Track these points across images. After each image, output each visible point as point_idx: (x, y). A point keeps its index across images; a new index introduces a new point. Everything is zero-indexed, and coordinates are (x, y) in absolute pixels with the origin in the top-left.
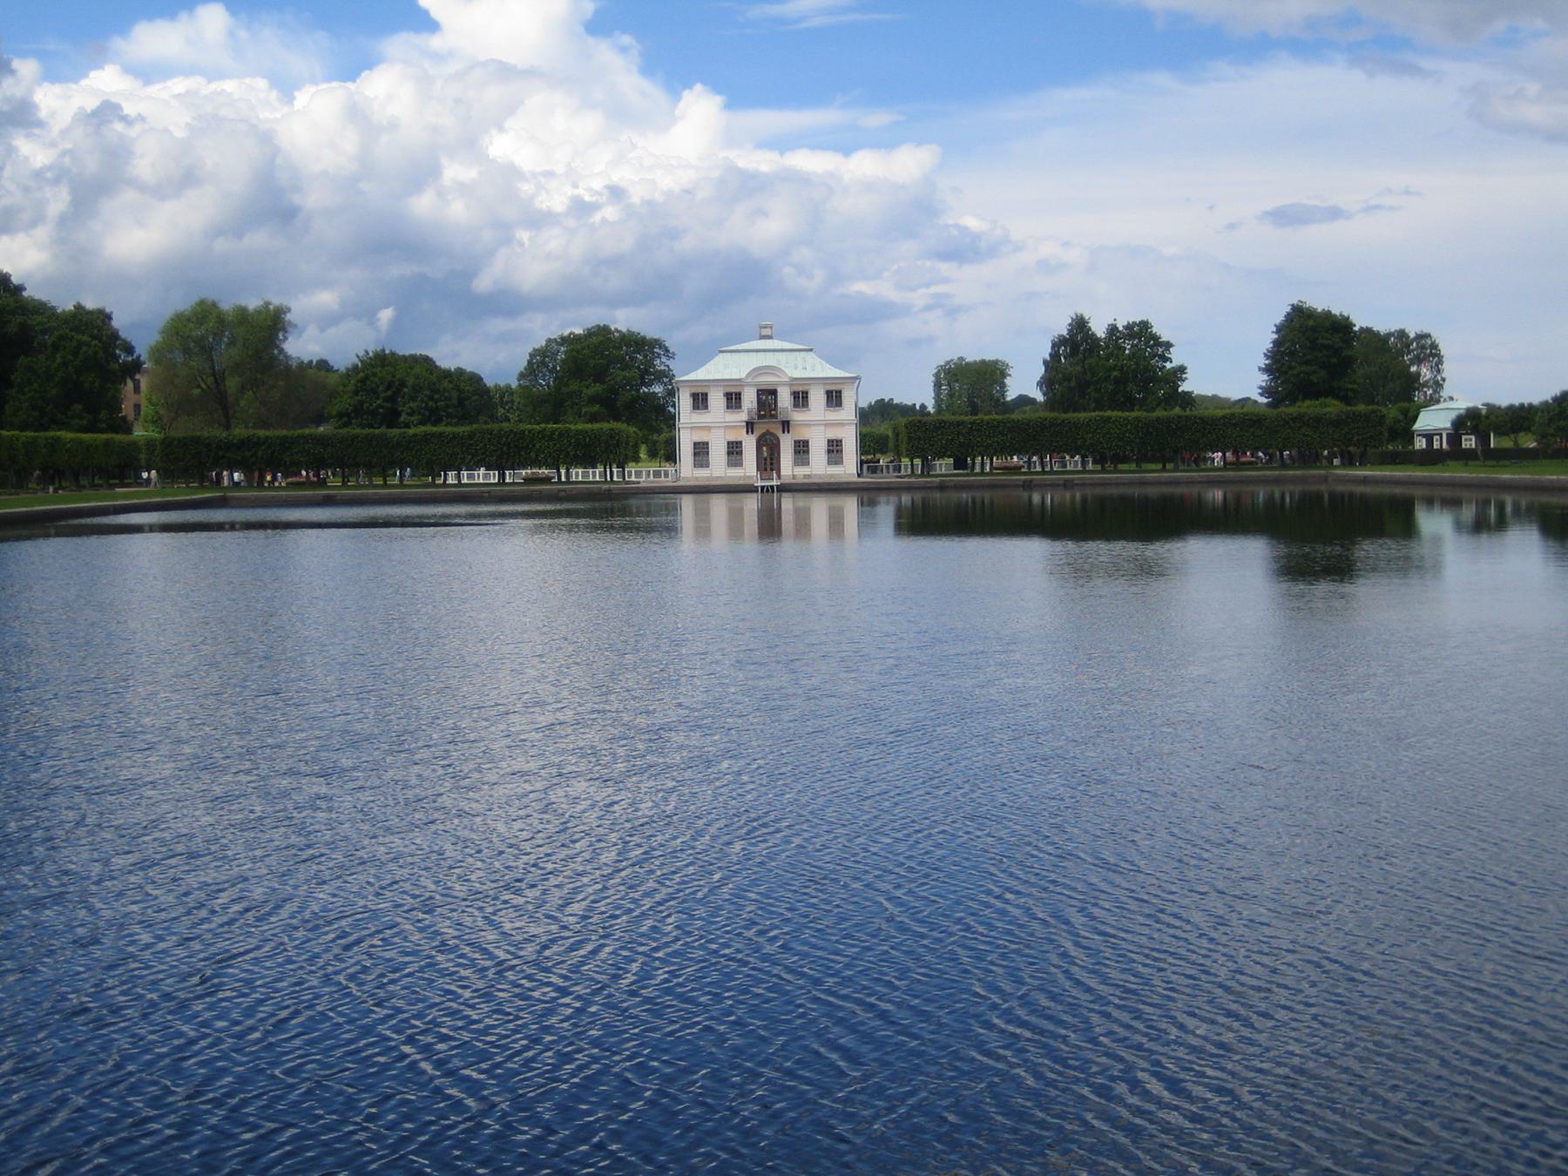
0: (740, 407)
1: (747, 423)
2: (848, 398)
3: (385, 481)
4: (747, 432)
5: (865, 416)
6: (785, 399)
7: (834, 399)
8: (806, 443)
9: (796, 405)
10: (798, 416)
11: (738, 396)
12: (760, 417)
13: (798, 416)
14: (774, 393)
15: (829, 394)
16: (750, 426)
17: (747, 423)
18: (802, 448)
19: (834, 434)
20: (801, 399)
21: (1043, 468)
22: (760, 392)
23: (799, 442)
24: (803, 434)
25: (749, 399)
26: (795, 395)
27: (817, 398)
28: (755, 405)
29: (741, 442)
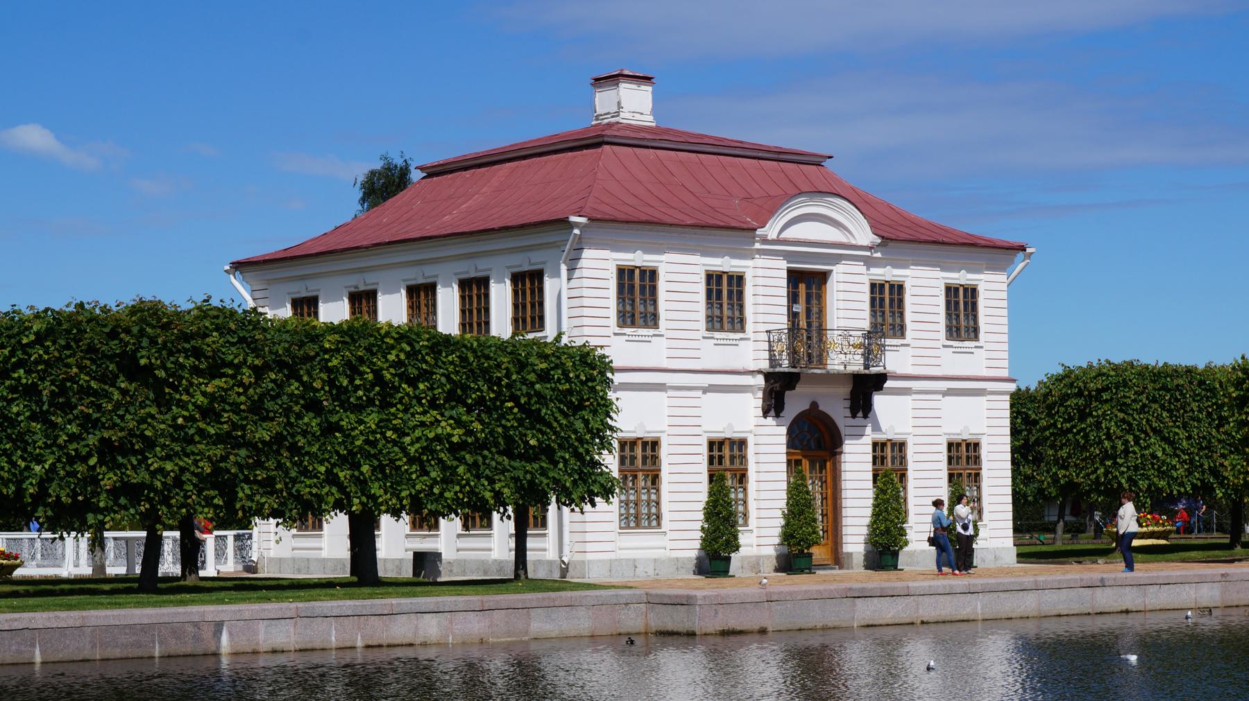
0: (738, 323)
13: (895, 359)
14: (821, 278)
17: (768, 376)
22: (795, 277)
29: (742, 443)
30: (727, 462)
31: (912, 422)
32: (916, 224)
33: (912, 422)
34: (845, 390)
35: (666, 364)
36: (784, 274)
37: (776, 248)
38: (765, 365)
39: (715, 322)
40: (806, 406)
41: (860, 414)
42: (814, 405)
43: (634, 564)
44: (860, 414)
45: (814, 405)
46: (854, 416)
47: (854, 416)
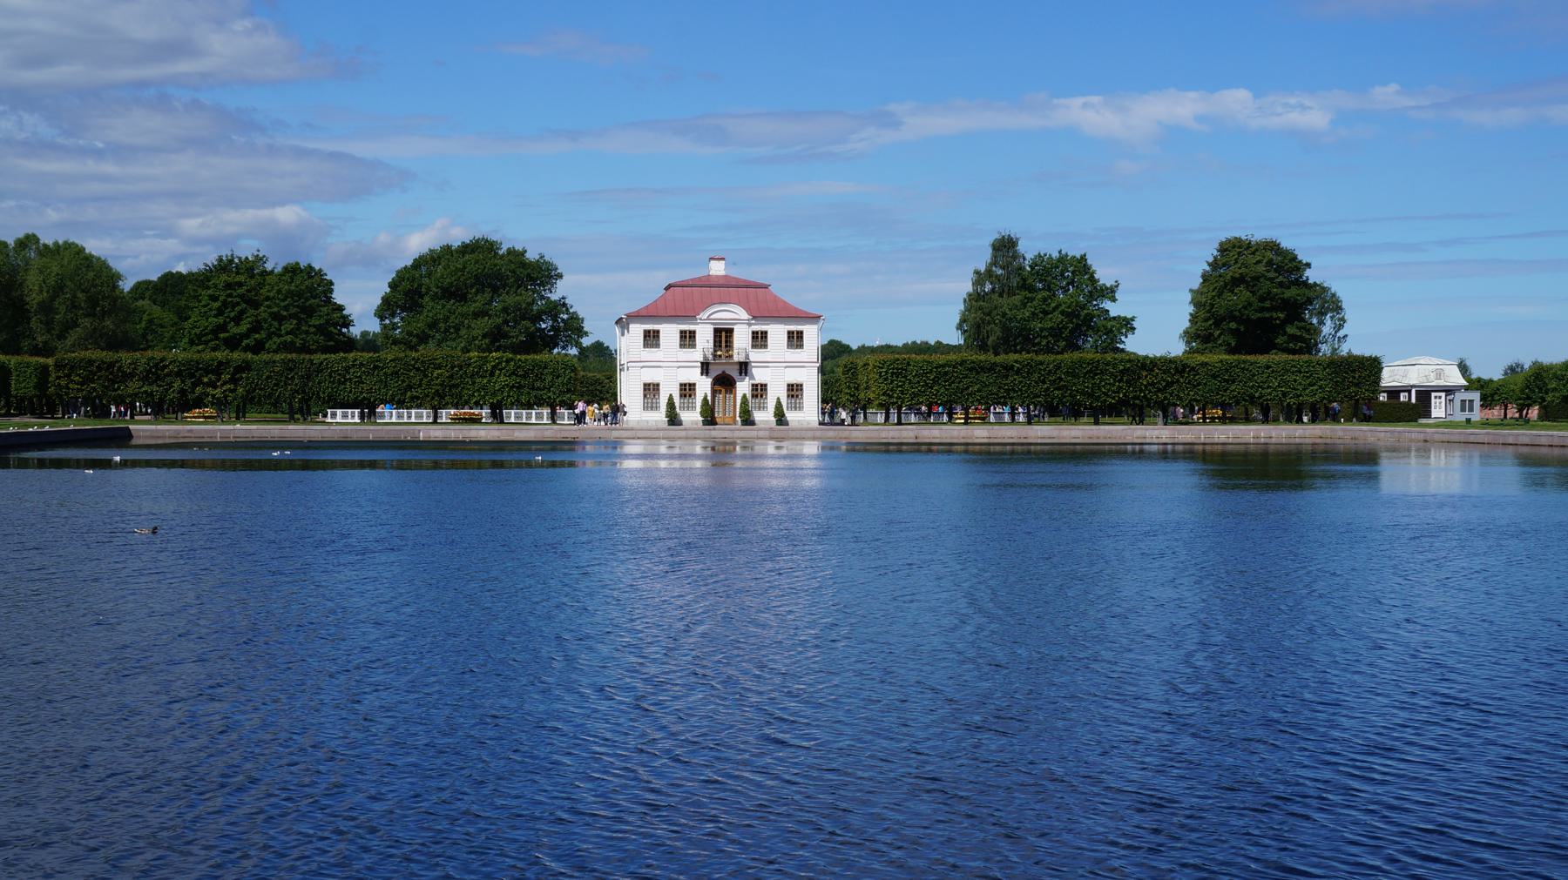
0: (693, 346)
4: (702, 374)
5: (832, 352)
6: (742, 339)
7: (795, 339)
8: (764, 387)
9: (754, 346)
10: (755, 356)
11: (692, 334)
12: (715, 356)
13: (755, 356)
14: (730, 332)
16: (705, 368)
17: (702, 363)
18: (760, 390)
19: (794, 376)
20: (759, 339)
22: (717, 332)
24: (759, 375)
26: (755, 335)
28: (711, 344)
32: (797, 310)
34: (737, 367)
36: (712, 330)
37: (706, 321)
38: (702, 360)
39: (682, 346)
40: (720, 372)
42: (724, 372)
43: (648, 422)
45: (724, 372)
46: (741, 374)
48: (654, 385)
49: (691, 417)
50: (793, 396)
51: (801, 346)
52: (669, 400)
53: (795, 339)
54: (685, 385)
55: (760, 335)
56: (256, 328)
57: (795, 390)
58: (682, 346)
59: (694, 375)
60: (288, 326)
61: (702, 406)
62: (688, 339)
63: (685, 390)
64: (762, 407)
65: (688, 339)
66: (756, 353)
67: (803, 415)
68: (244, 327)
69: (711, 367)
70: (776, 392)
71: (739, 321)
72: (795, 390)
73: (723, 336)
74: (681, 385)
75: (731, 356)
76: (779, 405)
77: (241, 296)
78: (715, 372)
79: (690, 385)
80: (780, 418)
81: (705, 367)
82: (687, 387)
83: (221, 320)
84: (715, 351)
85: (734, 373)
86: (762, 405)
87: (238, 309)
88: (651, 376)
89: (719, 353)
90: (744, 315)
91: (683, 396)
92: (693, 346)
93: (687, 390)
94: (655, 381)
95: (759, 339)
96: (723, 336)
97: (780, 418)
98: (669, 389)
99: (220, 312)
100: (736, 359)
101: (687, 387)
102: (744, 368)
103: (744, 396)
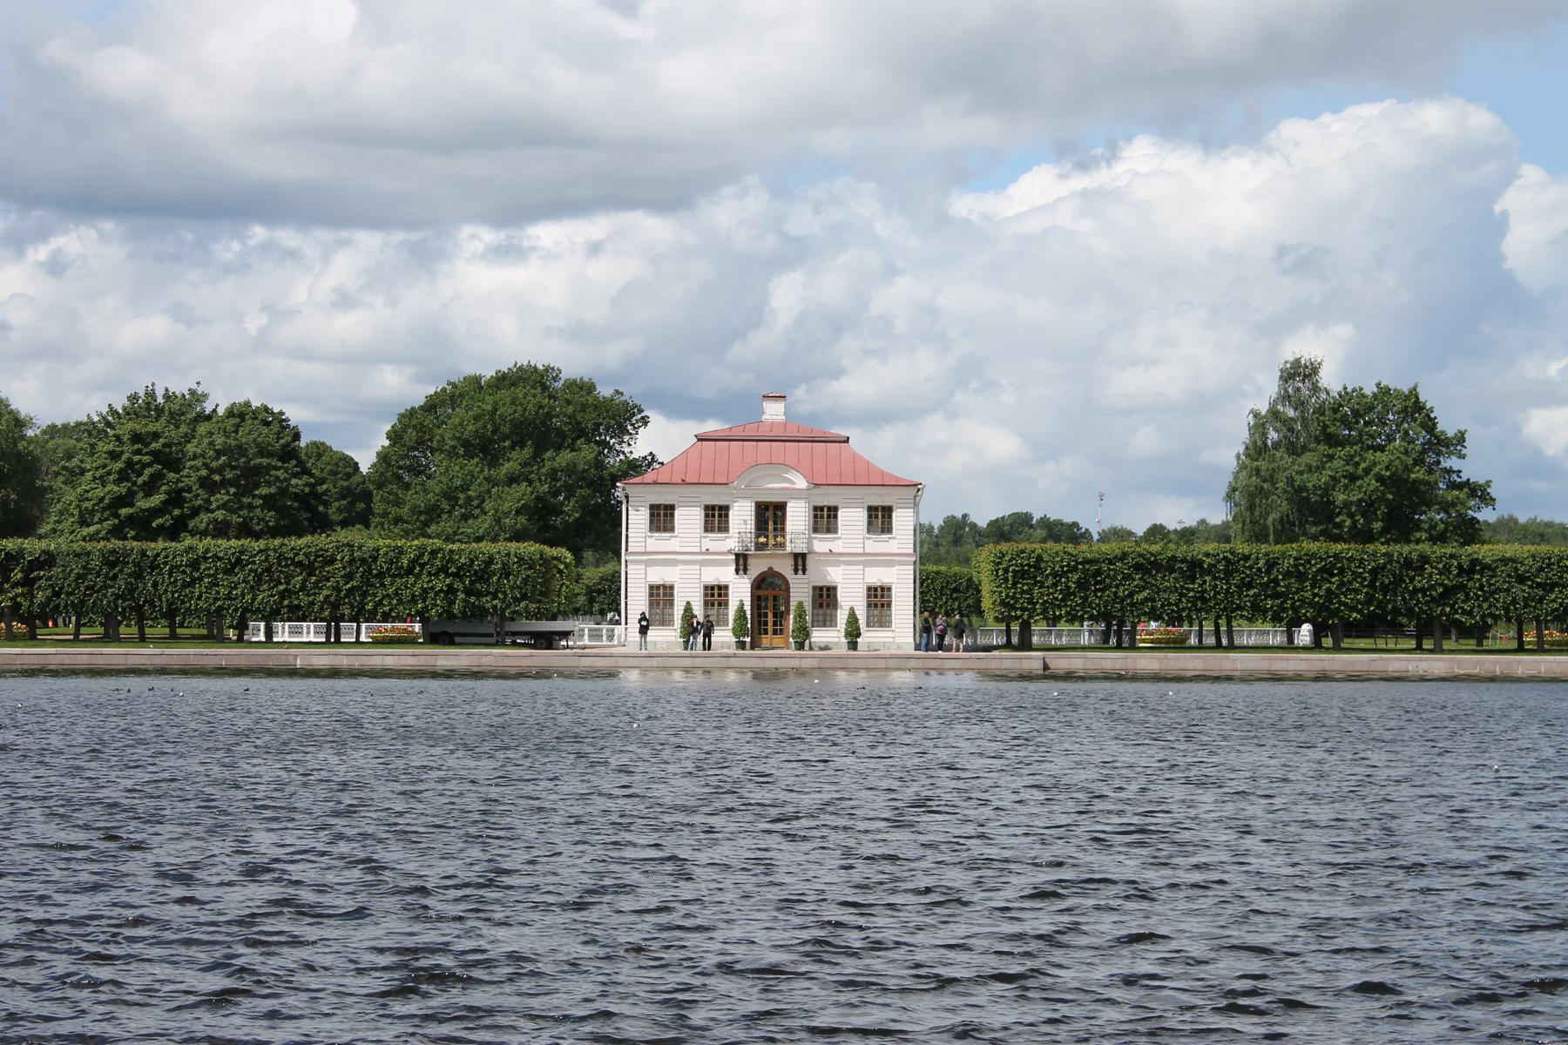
0: (726, 530)
1: (737, 555)
2: (903, 521)
3: (172, 627)
4: (737, 571)
6: (797, 518)
7: (880, 518)
11: (723, 511)
12: (760, 547)
14: (780, 508)
15: (872, 511)
16: (741, 562)
17: (737, 555)
18: (825, 597)
19: (877, 576)
20: (824, 518)
21: (1200, 641)
23: (821, 588)
25: (742, 516)
26: (817, 509)
27: (852, 519)
30: (716, 597)
31: (841, 576)
33: (841, 576)
35: (678, 550)
36: (753, 504)
39: (708, 528)
41: (800, 572)
42: (770, 568)
44: (800, 572)
45: (770, 568)
46: (796, 573)
47: (796, 573)
48: (665, 587)
49: (723, 636)
50: (876, 606)
51: (887, 528)
52: (685, 610)
53: (880, 518)
54: (712, 588)
55: (825, 513)
56: (176, 499)
57: (879, 598)
58: (708, 528)
59: (725, 574)
60: (221, 497)
61: (735, 620)
62: (716, 518)
63: (713, 595)
64: (828, 621)
65: (716, 518)
66: (821, 540)
67: (890, 634)
68: (156, 500)
69: (750, 561)
70: (851, 599)
71: (797, 494)
72: (879, 598)
73: (770, 515)
74: (706, 588)
75: (782, 545)
76: (853, 619)
77: (154, 454)
78: (757, 567)
79: (720, 588)
80: (853, 633)
81: (741, 561)
82: (716, 592)
83: (122, 489)
84: (758, 536)
85: (785, 568)
86: (828, 618)
87: (147, 472)
88: (658, 575)
89: (762, 540)
90: (801, 483)
91: (708, 604)
92: (724, 528)
93: (716, 595)
94: (668, 580)
95: (824, 518)
96: (770, 515)
97: (853, 633)
98: (688, 594)
99: (123, 476)
100: (789, 549)
101: (716, 592)
102: (800, 560)
103: (800, 604)
